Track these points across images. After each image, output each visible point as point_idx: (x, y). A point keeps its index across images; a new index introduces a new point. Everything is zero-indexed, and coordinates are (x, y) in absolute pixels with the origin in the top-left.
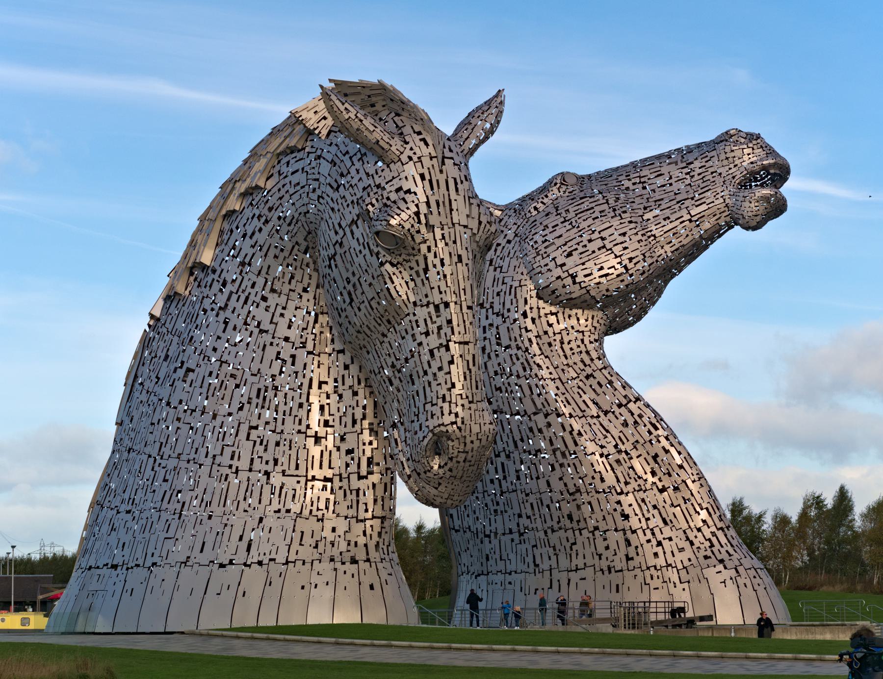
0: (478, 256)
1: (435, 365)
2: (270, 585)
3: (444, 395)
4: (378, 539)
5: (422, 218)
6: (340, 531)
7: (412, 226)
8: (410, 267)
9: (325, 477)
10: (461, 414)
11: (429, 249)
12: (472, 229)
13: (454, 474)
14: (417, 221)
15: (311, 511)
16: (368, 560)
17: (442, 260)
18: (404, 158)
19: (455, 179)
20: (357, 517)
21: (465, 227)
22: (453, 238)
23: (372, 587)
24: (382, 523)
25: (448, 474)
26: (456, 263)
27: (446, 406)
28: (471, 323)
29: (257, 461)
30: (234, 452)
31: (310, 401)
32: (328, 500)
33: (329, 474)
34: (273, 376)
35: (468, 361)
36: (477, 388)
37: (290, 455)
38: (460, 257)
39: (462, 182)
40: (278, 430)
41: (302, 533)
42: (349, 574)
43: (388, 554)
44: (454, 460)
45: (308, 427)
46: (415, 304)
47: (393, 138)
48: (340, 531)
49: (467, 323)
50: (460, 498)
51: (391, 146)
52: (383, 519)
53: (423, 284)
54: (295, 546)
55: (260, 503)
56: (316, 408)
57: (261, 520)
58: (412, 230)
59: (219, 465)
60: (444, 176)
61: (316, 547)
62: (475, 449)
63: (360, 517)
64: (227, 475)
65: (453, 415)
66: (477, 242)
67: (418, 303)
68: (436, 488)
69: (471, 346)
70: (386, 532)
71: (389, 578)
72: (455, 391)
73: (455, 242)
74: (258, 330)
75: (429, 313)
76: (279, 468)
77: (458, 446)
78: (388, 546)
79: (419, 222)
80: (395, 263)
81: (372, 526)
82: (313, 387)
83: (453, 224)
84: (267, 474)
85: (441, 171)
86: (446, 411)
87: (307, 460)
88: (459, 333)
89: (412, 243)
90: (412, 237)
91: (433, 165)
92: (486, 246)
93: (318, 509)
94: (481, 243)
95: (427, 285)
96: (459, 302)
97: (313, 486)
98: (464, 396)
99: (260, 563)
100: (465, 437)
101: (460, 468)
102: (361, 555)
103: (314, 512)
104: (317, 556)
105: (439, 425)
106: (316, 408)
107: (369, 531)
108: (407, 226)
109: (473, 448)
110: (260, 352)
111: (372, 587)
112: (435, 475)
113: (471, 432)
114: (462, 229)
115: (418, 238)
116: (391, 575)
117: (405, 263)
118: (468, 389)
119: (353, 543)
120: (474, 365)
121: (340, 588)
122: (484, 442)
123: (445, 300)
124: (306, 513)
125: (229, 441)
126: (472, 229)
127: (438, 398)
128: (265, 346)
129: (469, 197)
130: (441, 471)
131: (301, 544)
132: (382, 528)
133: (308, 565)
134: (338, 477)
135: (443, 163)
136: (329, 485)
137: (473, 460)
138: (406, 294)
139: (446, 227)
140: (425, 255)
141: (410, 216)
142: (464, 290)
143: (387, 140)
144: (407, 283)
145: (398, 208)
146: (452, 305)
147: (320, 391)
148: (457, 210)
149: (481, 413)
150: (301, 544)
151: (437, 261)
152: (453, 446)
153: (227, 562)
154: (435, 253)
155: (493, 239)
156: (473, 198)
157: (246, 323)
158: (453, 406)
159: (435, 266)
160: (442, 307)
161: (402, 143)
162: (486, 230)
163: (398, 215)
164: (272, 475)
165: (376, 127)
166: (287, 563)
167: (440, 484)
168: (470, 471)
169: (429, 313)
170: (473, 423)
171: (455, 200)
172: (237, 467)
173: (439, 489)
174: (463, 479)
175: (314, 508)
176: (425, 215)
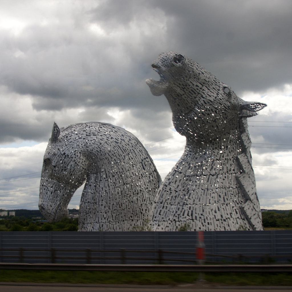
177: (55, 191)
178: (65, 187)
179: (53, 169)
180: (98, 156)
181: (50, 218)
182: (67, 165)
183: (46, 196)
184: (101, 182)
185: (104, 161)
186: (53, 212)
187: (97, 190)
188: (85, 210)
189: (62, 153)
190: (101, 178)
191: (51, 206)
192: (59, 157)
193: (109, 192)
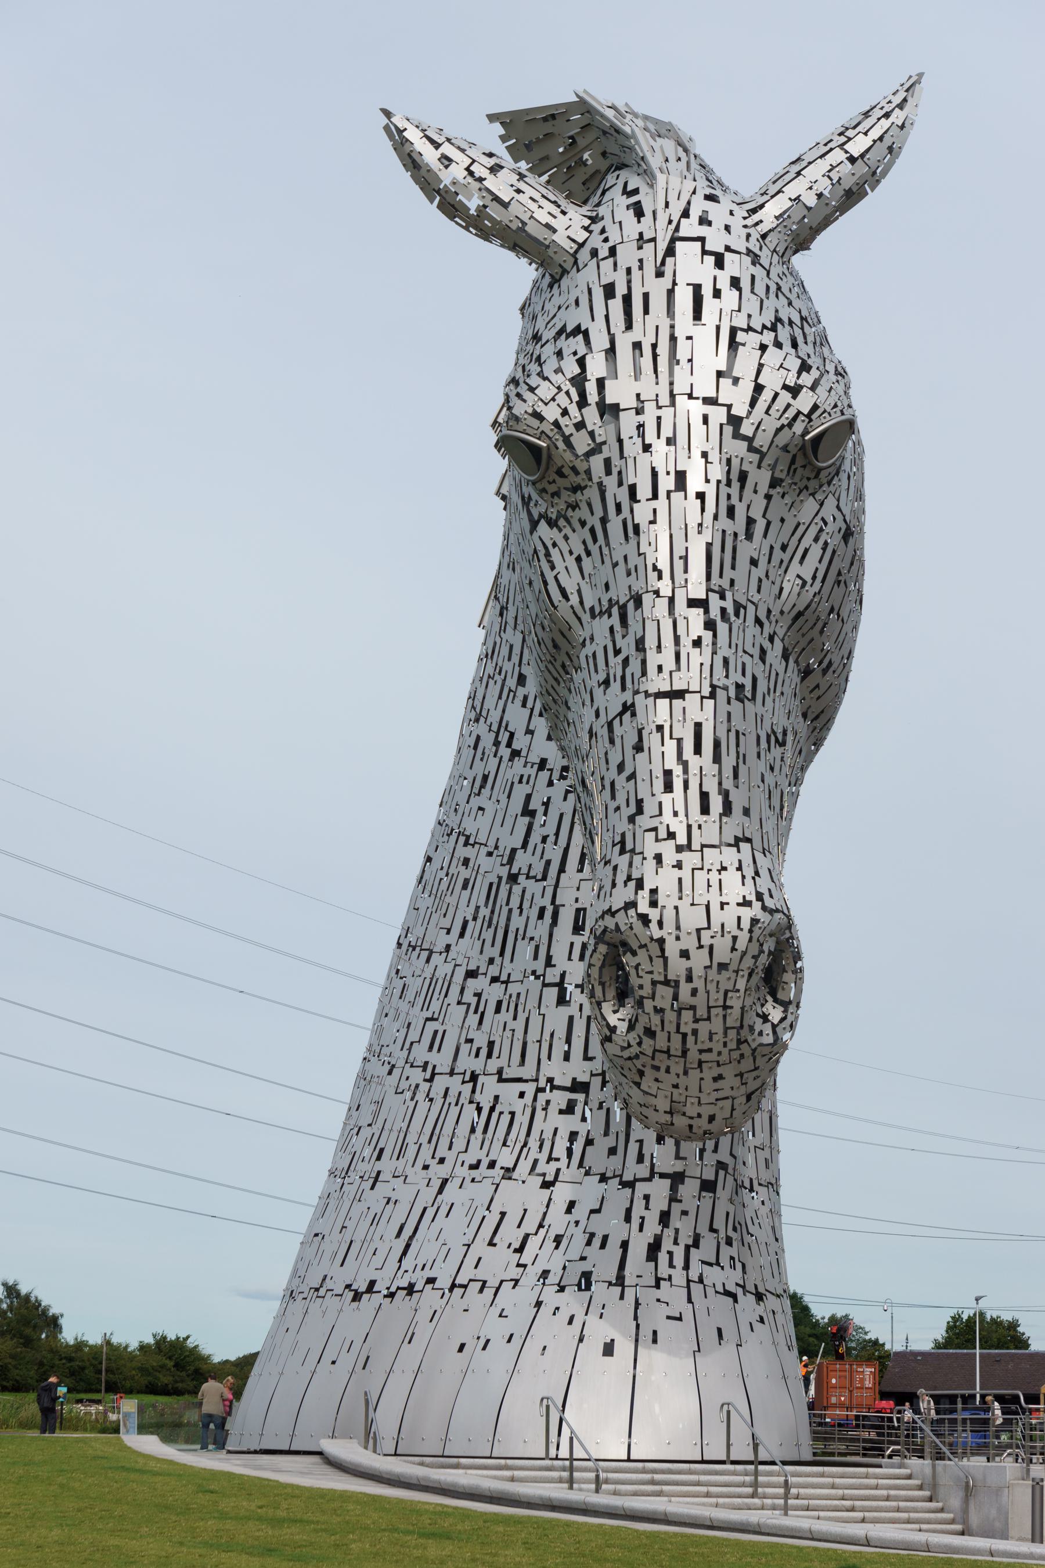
0: (761, 478)
1: (615, 758)
2: (410, 1342)
3: (623, 835)
4: (658, 1229)
5: (591, 388)
6: (580, 1212)
7: (565, 412)
8: (580, 520)
9: (574, 1079)
10: (648, 885)
11: (608, 462)
12: (729, 407)
13: (661, 1042)
14: (575, 397)
15: (536, 1161)
16: (620, 1281)
17: (633, 489)
18: (584, 255)
19: (697, 288)
20: (621, 1176)
21: (709, 401)
22: (667, 431)
23: (609, 1349)
24: (674, 1188)
25: (647, 1042)
26: (669, 493)
27: (623, 861)
28: (697, 643)
29: (465, 1048)
30: (436, 1032)
31: (557, 903)
32: (573, 1136)
33: (578, 1069)
34: (514, 851)
35: (680, 741)
36: (705, 810)
37: (514, 1030)
38: (681, 478)
39: (717, 293)
40: (504, 978)
41: (503, 1214)
42: (564, 1316)
43: (686, 1267)
44: (648, 1004)
45: (549, 963)
46: (592, 609)
47: (564, 213)
48: (580, 1212)
49: (686, 642)
50: (706, 1111)
51: (555, 231)
52: (677, 1179)
53: (603, 562)
54: (480, 1247)
55: (450, 1148)
56: (566, 918)
57: (440, 1191)
58: (563, 421)
59: (412, 1066)
60: (666, 282)
61: (520, 1250)
62: (698, 972)
63: (628, 1177)
64: (417, 1086)
65: (632, 884)
66: (750, 440)
67: (597, 610)
68: (638, 1085)
69: (692, 700)
70: (685, 1213)
71: (666, 1329)
72: (644, 821)
73: (671, 441)
74: (509, 750)
75: (612, 629)
76: (493, 1065)
77: (650, 969)
78: (687, 1248)
79: (583, 403)
80: (554, 517)
81: (647, 1198)
82: (567, 868)
83: (672, 396)
84: (474, 1078)
85: (659, 274)
86: (621, 878)
87: (540, 1041)
88: (660, 668)
89: (568, 456)
90: (567, 440)
91: (641, 261)
92: (785, 449)
93: (550, 1159)
94: (762, 441)
95: (607, 559)
96: (666, 590)
97: (548, 1102)
98: (662, 834)
99: (410, 1289)
100: (661, 941)
101: (671, 1027)
102: (605, 1264)
103: (541, 1168)
104: (514, 1272)
105: (602, 917)
106: (566, 918)
107: (638, 1210)
108: (551, 413)
109: (690, 970)
110: (503, 798)
111: (609, 1349)
112: (623, 1049)
113: (678, 928)
114: (697, 408)
115: (582, 443)
116: (680, 1319)
117: (570, 513)
118: (676, 814)
119: (597, 1242)
120: (698, 750)
121: (533, 1346)
122: (722, 954)
123: (635, 588)
124: (524, 1166)
125: (435, 1006)
126: (729, 407)
127: (614, 845)
128: (513, 783)
129: (733, 331)
130: (633, 1038)
131: (491, 1244)
132: (673, 1199)
133: (489, 1292)
134: (600, 1078)
135: (670, 252)
136: (580, 1097)
137: (700, 1002)
138: (579, 592)
139: (650, 407)
140: (600, 484)
141: (559, 388)
142: (685, 558)
143: (544, 218)
144: (579, 559)
145: (541, 374)
146: (647, 599)
147: (581, 876)
148: (690, 360)
149: (714, 877)
150: (491, 1244)
151: (623, 495)
152: (637, 967)
153: (363, 1288)
154: (620, 473)
155: (806, 432)
156: (749, 329)
157: (497, 743)
158: (637, 859)
159: (619, 507)
160: (631, 606)
161: (587, 222)
162: (780, 404)
163: (532, 390)
164: (481, 1079)
165: (518, 191)
166: (453, 1286)
167: (641, 1073)
168: (703, 1035)
169: (612, 629)
170: (684, 905)
171: (689, 338)
172: (434, 1067)
173: (644, 1087)
174: (693, 1055)
175: (543, 1156)
176: (601, 383)
179: (834, 552)
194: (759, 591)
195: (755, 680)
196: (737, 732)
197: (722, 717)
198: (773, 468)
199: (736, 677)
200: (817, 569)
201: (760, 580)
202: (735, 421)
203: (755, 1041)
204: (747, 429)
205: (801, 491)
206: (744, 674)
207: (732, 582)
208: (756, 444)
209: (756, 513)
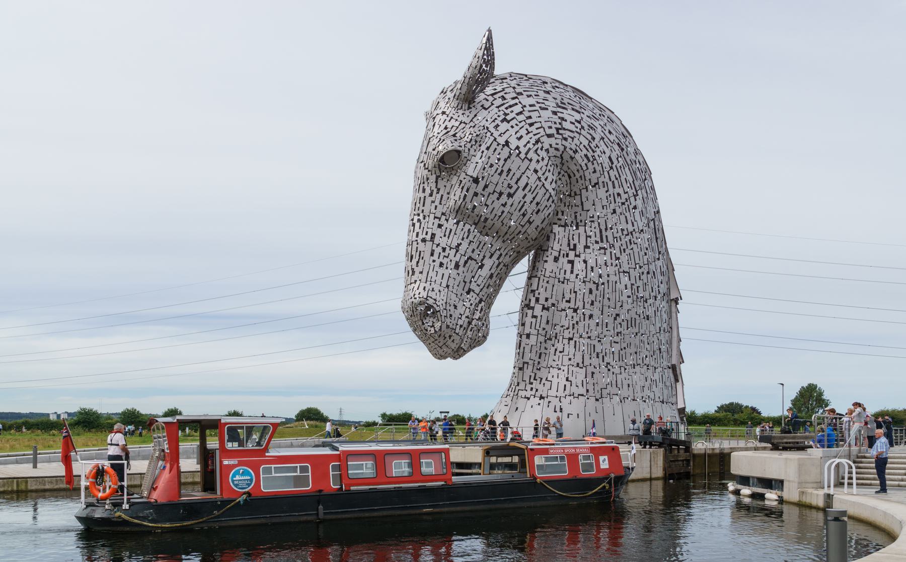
66: (427, 168)
177: (466, 262)
178: (498, 253)
180: (587, 173)
181: (449, 342)
182: (515, 179)
183: (440, 275)
184: (586, 250)
185: (598, 190)
186: (461, 326)
187: (575, 272)
188: (544, 329)
189: (502, 141)
190: (588, 242)
191: (455, 307)
192: (492, 149)
193: (608, 281)
194: (436, 209)
195: (433, 235)
196: (420, 252)
197: (414, 249)
198: (435, 173)
199: (421, 237)
200: (460, 195)
201: (436, 207)
202: (425, 165)
203: (429, 333)
204: (426, 167)
205: (450, 176)
206: (426, 234)
207: (423, 211)
208: (429, 169)
209: (434, 188)
